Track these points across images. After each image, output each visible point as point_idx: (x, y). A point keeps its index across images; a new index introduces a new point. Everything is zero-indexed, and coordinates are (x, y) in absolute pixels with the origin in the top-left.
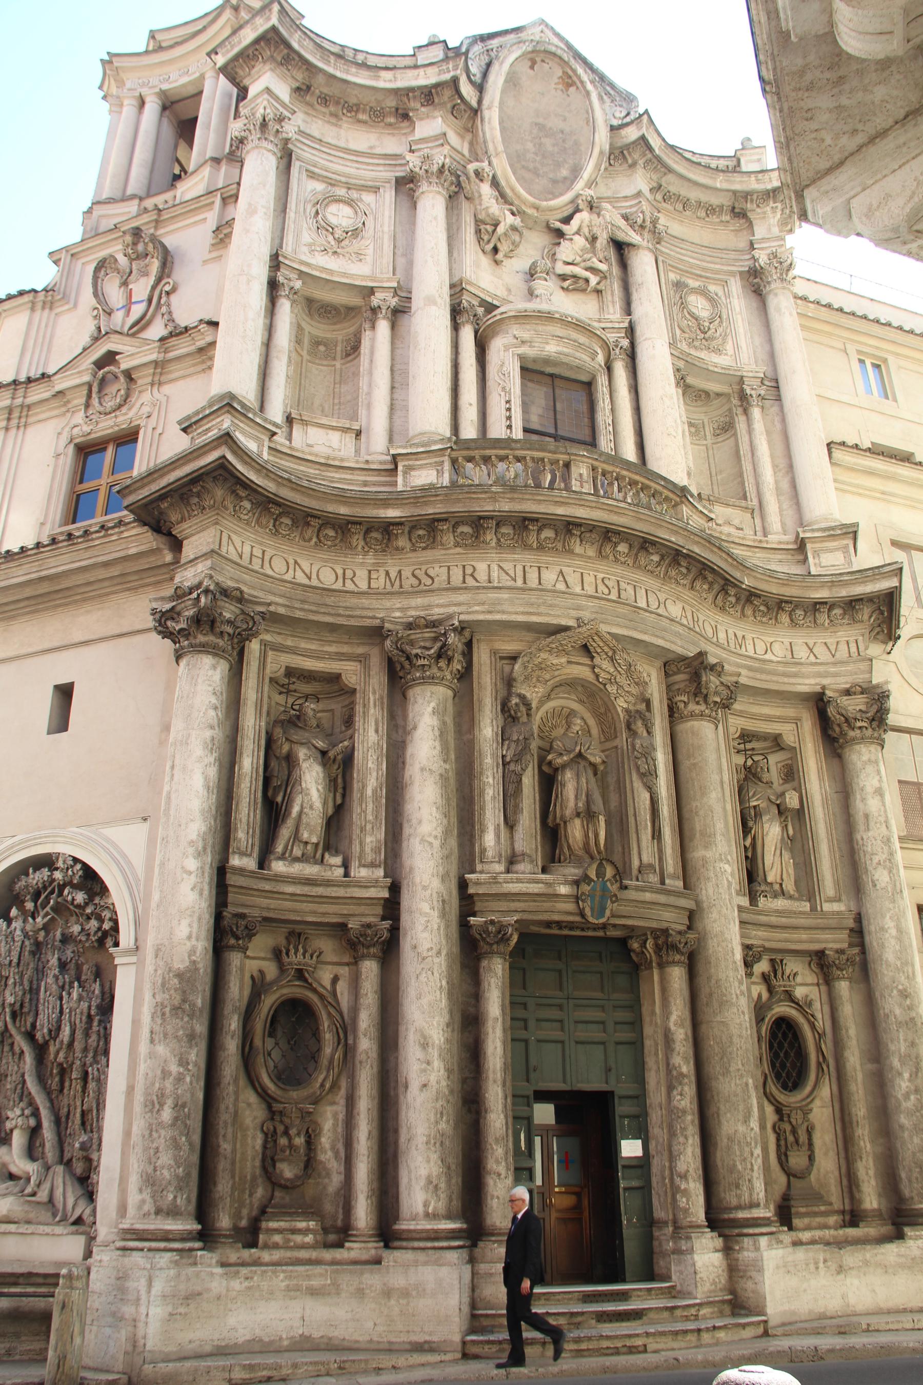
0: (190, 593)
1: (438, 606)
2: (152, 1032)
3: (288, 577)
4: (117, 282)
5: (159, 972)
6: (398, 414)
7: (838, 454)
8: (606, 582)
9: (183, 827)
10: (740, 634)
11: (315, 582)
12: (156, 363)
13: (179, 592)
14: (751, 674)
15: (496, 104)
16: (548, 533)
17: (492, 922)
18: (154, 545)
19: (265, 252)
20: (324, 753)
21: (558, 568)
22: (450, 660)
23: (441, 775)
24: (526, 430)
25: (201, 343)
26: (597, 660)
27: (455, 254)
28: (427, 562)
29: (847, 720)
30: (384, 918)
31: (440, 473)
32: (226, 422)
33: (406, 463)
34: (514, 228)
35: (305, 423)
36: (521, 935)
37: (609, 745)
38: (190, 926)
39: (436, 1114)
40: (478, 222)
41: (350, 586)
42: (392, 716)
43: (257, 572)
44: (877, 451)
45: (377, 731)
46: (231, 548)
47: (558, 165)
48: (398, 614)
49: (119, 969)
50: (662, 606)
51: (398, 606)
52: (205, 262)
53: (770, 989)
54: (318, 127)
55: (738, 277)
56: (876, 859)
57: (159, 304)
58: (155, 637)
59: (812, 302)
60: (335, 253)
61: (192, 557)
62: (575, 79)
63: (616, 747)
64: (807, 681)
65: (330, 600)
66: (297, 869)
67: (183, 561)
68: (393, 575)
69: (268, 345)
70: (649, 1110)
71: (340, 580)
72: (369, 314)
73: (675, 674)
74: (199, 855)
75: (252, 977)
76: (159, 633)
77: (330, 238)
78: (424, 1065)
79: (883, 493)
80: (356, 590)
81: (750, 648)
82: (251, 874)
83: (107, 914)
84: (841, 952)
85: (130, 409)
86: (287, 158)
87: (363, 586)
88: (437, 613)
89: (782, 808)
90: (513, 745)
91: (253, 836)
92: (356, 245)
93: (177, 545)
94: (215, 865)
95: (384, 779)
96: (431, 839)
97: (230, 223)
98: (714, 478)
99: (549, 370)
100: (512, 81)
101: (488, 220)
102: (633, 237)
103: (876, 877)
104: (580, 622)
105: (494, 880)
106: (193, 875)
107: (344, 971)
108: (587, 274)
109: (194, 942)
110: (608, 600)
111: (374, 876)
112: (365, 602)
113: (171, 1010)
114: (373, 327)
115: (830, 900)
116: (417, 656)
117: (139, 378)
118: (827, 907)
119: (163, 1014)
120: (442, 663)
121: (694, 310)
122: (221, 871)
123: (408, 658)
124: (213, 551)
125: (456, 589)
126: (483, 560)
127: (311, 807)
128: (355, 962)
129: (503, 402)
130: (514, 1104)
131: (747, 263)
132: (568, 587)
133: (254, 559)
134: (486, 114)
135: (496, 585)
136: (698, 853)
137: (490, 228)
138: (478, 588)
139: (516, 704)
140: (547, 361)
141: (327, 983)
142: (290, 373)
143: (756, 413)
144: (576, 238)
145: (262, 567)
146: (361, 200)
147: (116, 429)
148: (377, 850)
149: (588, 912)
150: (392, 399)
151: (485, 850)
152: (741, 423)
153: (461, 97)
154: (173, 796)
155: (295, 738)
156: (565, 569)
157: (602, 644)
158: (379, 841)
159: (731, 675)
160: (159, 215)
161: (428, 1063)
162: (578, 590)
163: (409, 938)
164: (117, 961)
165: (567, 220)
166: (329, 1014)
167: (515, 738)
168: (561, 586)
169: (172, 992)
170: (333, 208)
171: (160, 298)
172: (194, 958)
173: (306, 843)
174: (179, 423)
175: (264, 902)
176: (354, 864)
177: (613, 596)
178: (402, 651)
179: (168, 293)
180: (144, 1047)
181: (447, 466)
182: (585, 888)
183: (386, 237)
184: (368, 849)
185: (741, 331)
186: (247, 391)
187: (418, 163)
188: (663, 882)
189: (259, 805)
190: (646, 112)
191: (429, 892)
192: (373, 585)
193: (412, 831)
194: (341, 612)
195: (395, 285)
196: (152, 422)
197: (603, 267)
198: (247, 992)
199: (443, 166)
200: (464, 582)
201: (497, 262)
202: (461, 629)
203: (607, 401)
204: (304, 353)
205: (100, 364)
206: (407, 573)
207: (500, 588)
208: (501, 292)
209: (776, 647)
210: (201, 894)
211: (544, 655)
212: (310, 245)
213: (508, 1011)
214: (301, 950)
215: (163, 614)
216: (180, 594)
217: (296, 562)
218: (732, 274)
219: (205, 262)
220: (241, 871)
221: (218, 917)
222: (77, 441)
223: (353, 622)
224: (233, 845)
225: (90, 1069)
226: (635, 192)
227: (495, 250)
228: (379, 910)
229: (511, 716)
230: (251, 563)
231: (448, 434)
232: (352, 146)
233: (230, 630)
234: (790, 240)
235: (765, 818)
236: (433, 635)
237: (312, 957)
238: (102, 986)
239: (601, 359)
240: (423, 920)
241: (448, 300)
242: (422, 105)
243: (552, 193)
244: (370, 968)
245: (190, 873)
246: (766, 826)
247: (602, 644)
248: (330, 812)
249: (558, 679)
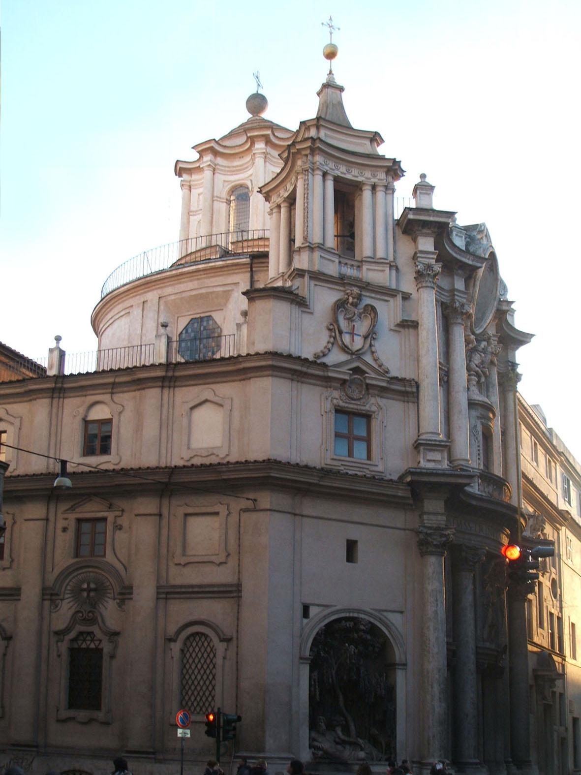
4: (343, 314)
12: (382, 387)
25: (408, 389)
52: (391, 330)
61: (431, 510)
147: (360, 411)
154: (439, 612)
160: (367, 286)
171: (371, 340)
179: (374, 338)
219: (391, 330)
222: (336, 407)
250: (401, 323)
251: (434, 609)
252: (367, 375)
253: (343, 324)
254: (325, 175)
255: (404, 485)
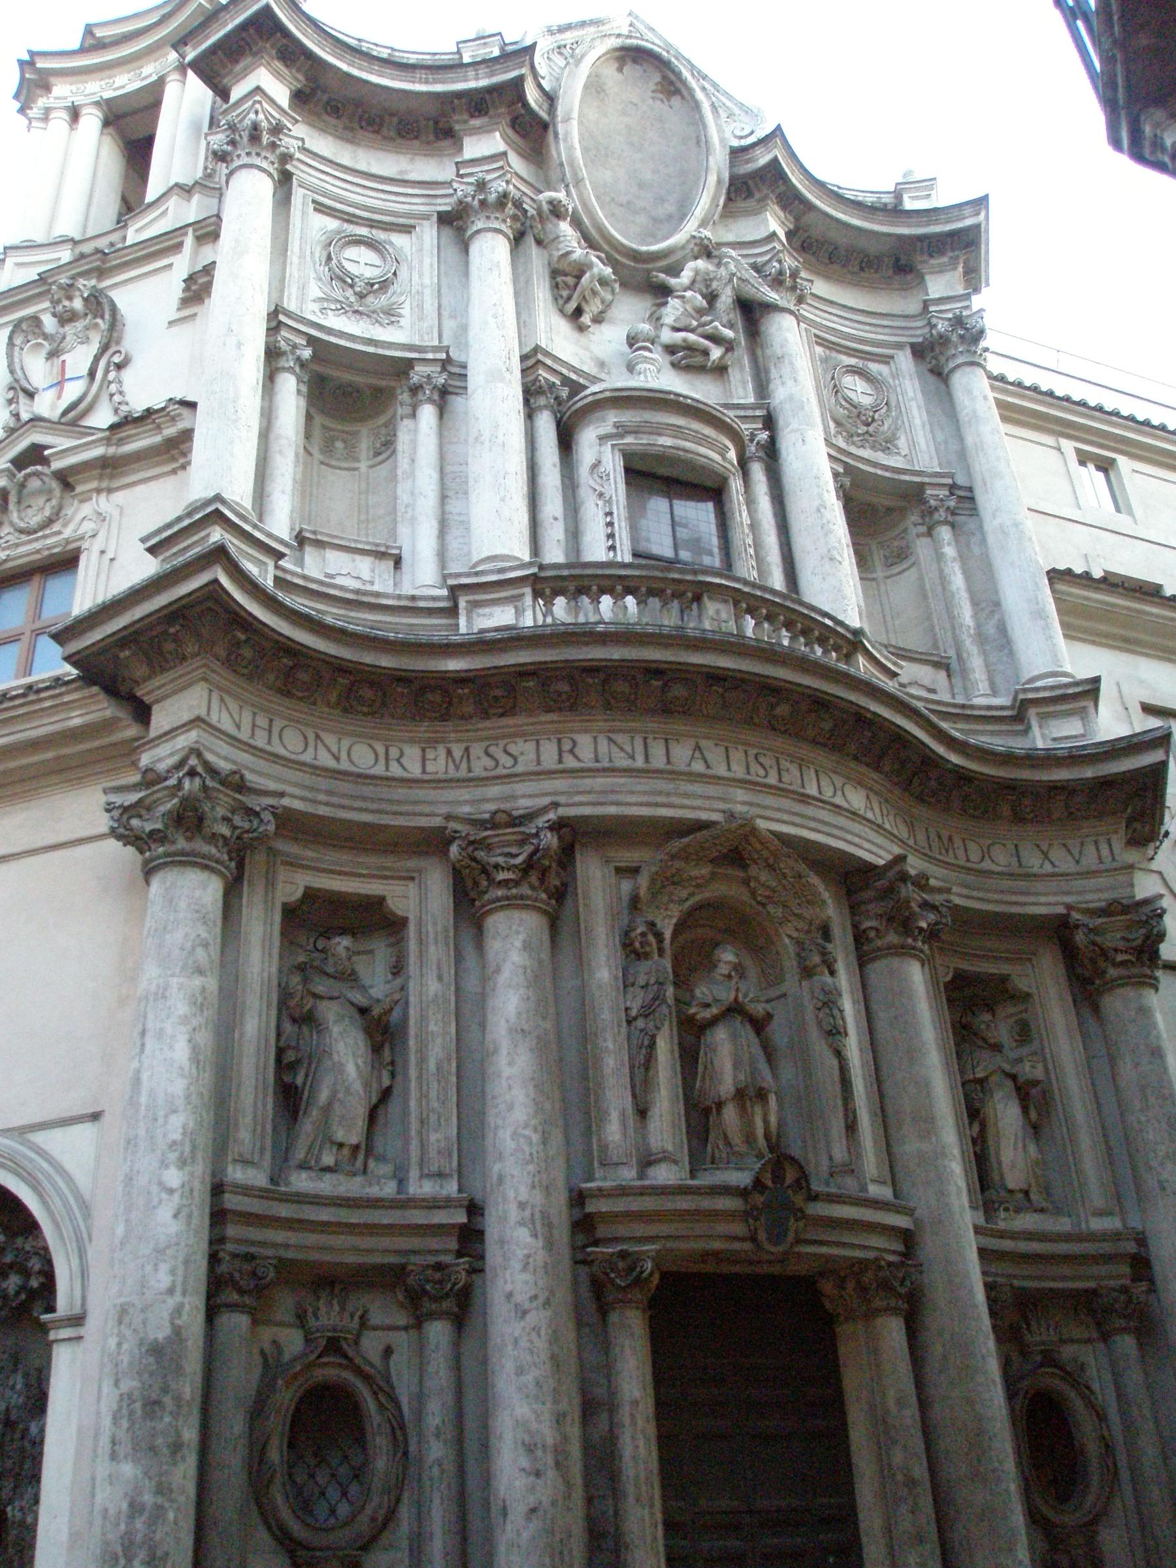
0: (166, 779)
1: (523, 796)
2: (114, 1443)
3: (307, 757)
5: (125, 1346)
6: (454, 534)
7: (1060, 587)
8: (762, 759)
9: (161, 1121)
10: (945, 834)
11: (345, 765)
13: (150, 776)
14: (965, 891)
15: (575, 115)
16: (678, 691)
17: (623, 1255)
18: (108, 713)
19: (261, 309)
20: (363, 1011)
21: (692, 742)
22: (544, 873)
23: (538, 1037)
24: (636, 555)
25: (170, 431)
26: (753, 870)
27: (524, 317)
28: (503, 737)
29: (1104, 953)
30: (460, 1254)
31: (519, 612)
32: (217, 535)
33: (471, 598)
34: (603, 282)
35: (320, 544)
36: (664, 1276)
37: (773, 993)
38: (173, 1272)
39: (552, 1556)
40: (555, 273)
41: (395, 770)
42: (459, 959)
43: (261, 750)
44: (1112, 583)
45: (440, 978)
46: (225, 716)
47: (662, 200)
48: (467, 809)
49: (55, 1346)
50: (839, 793)
51: (467, 797)
52: (171, 323)
53: (1024, 1352)
54: (323, 145)
55: (908, 351)
56: (1162, 1150)
57: (106, 382)
58: (113, 845)
59: (1012, 384)
60: (356, 312)
61: (167, 728)
62: (679, 85)
63: (784, 995)
64: (1043, 899)
65: (368, 790)
66: (326, 1185)
67: (153, 733)
68: (458, 752)
69: (265, 435)
70: (864, 1540)
71: (382, 761)
72: (405, 397)
73: (861, 889)
74: (182, 1163)
75: (263, 1353)
76: (119, 837)
77: (349, 292)
78: (532, 1478)
79: (1126, 640)
80: (405, 775)
81: (961, 853)
82: (263, 1194)
83: (35, 1264)
84: (1124, 1290)
85: (65, 525)
86: (284, 180)
87: (415, 771)
88: (524, 805)
89: (1021, 1080)
90: (641, 994)
91: (263, 1137)
92: (383, 300)
93: (142, 713)
94: (208, 1179)
95: (453, 1046)
96: (527, 1132)
97: (209, 269)
98: (890, 624)
99: (663, 471)
100: (594, 87)
101: (567, 269)
102: (772, 296)
103: (1165, 1176)
104: (731, 815)
105: (622, 1191)
106: (176, 1196)
107: (400, 1340)
108: (706, 342)
109: (178, 1298)
110: (765, 785)
111: (444, 1192)
112: (420, 793)
113: (144, 1406)
114: (413, 415)
115: (1101, 1213)
116: (497, 866)
117: (79, 482)
118: (1097, 1224)
119: (131, 1413)
120: (534, 878)
121: (852, 395)
122: (218, 1189)
123: (484, 871)
124: (198, 719)
125: (550, 773)
126: (586, 731)
127: (348, 1091)
128: (418, 1323)
129: (601, 514)
130: (666, 1537)
131: (919, 332)
132: (708, 767)
133: (258, 732)
134: (561, 129)
135: (606, 764)
136: (910, 1146)
137: (570, 280)
138: (582, 770)
139: (643, 935)
140: (662, 458)
141: (375, 1357)
142: (299, 476)
143: (945, 533)
144: (689, 294)
145: (269, 743)
146: (391, 243)
147: (46, 553)
148: (445, 1153)
149: (762, 1236)
150: (443, 513)
151: (607, 1146)
152: (922, 548)
153: (526, 105)
154: (145, 1076)
155: (320, 989)
156: (704, 743)
157: (758, 846)
158: (447, 1138)
159: (940, 890)
160: (104, 262)
161: (538, 1474)
162: (722, 771)
163: (500, 1282)
164: (52, 1336)
165: (675, 271)
166: (381, 1406)
167: (641, 981)
168: (698, 767)
169: (146, 1376)
170: (352, 252)
171: (107, 372)
172: (178, 1322)
173: (341, 1145)
174: (143, 540)
175: (279, 1236)
176: (414, 1173)
177: (772, 780)
178: (474, 859)
180: (103, 1468)
181: (528, 600)
182: (759, 1199)
183: (427, 292)
184: (433, 1153)
185: (918, 422)
186: (240, 492)
187: (470, 190)
188: (864, 1188)
189: (271, 1090)
190: (779, 128)
191: (527, 1213)
192: (430, 767)
193: (500, 1122)
194: (384, 806)
195: (444, 356)
196: (97, 545)
197: (729, 333)
198: (256, 1373)
199: (505, 195)
200: (560, 761)
201: (581, 329)
202: (558, 826)
203: (745, 514)
204: (315, 451)
205: (20, 462)
206: (477, 750)
207: (613, 770)
208: (589, 367)
209: (997, 851)
210: (189, 1224)
211: (678, 864)
212: (321, 300)
213: (650, 1391)
214: (337, 1308)
215: (125, 809)
216: (151, 779)
217: (317, 736)
218: (899, 346)
219: (171, 323)
220: (246, 1190)
221: (214, 1259)
223: (402, 821)
224: (233, 1151)
225: (9, 1509)
226: (765, 234)
227: (579, 312)
228: (453, 1245)
229: (635, 952)
230: (253, 736)
231: (527, 558)
232: (375, 170)
233: (225, 830)
234: (977, 302)
235: (998, 1095)
236: (519, 837)
237: (352, 1316)
238: (26, 1375)
239: (732, 455)
240: (520, 1253)
241: (519, 375)
242: (472, 116)
243: (653, 236)
244: (438, 1332)
245: (171, 1191)
246: (1000, 1107)
247: (758, 846)
248: (374, 1100)
249: (697, 898)
250: (188, 294)
251: (135, 1064)
252: (46, 453)
253: (37, 369)
254: (75, 114)
255: (73, 686)
